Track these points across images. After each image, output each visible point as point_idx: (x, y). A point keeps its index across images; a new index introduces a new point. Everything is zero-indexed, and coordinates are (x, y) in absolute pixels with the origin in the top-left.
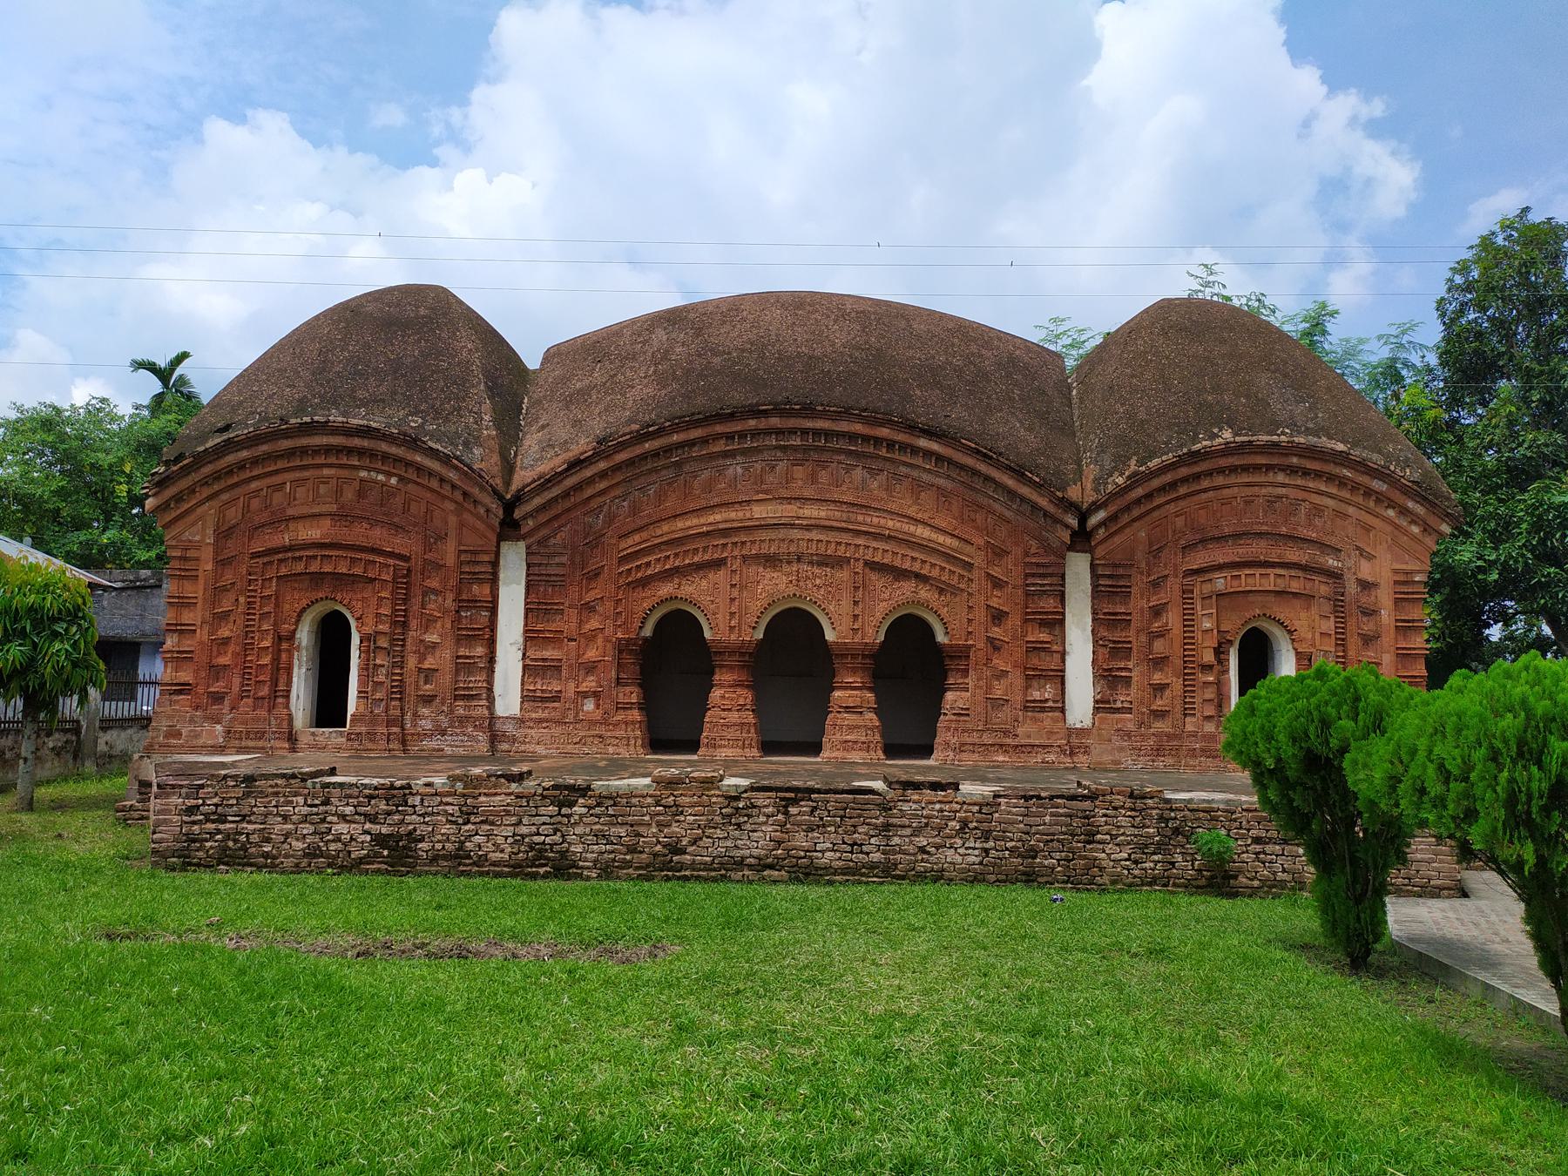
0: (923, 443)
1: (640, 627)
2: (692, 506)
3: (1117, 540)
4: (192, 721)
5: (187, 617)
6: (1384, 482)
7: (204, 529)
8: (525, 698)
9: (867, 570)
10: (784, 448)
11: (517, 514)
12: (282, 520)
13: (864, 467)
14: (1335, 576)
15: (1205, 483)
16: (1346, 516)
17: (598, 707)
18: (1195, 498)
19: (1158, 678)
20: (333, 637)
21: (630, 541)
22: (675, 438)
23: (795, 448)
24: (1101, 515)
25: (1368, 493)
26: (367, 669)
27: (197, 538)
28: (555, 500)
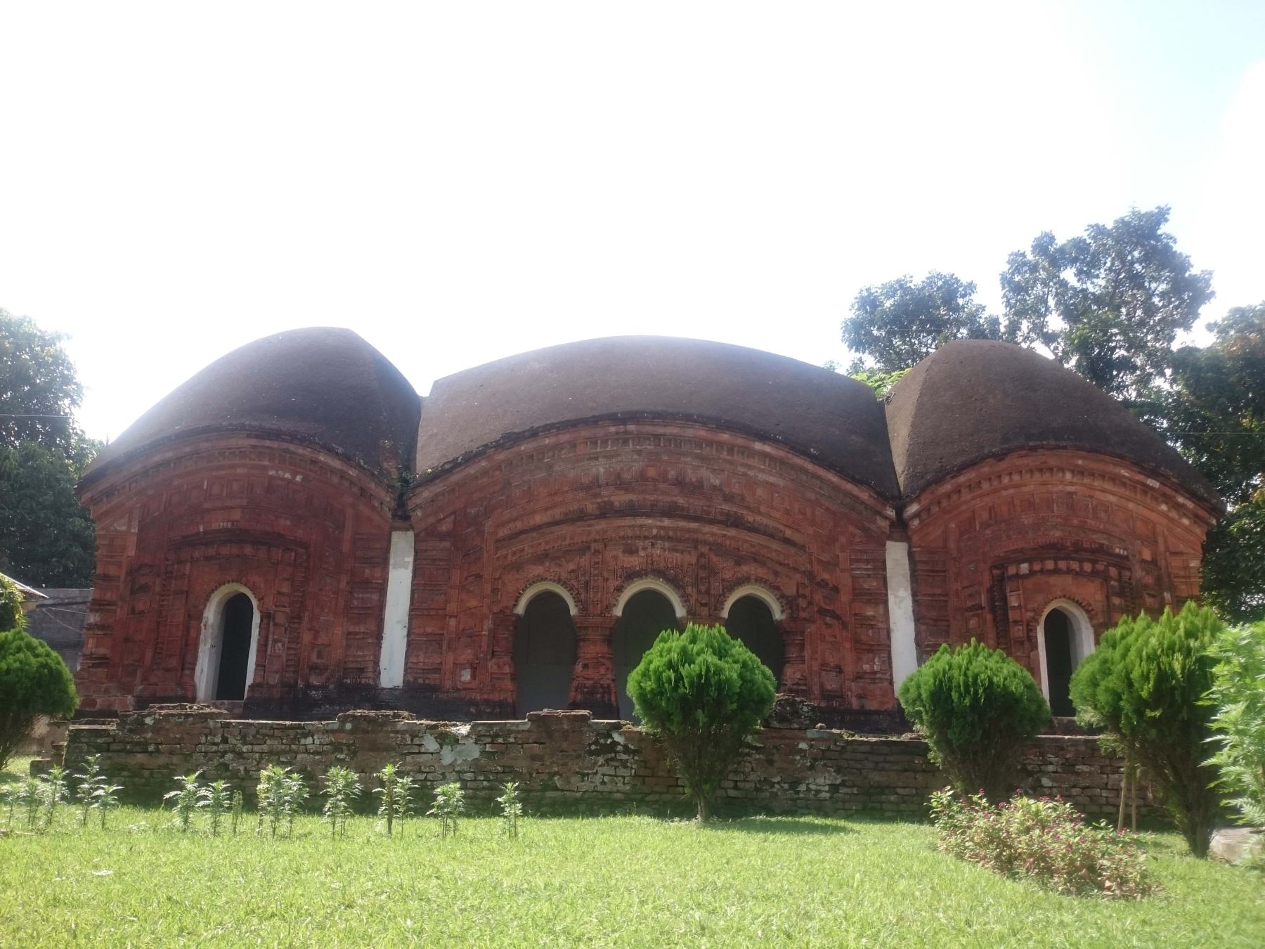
0: (758, 446)
1: (515, 606)
6: (1158, 481)
7: (130, 521)
8: (407, 669)
9: (712, 556)
11: (410, 505)
13: (707, 468)
14: (1122, 563)
16: (1126, 509)
17: (474, 677)
22: (547, 441)
24: (914, 508)
25: (1146, 489)
26: (266, 645)
27: (124, 528)
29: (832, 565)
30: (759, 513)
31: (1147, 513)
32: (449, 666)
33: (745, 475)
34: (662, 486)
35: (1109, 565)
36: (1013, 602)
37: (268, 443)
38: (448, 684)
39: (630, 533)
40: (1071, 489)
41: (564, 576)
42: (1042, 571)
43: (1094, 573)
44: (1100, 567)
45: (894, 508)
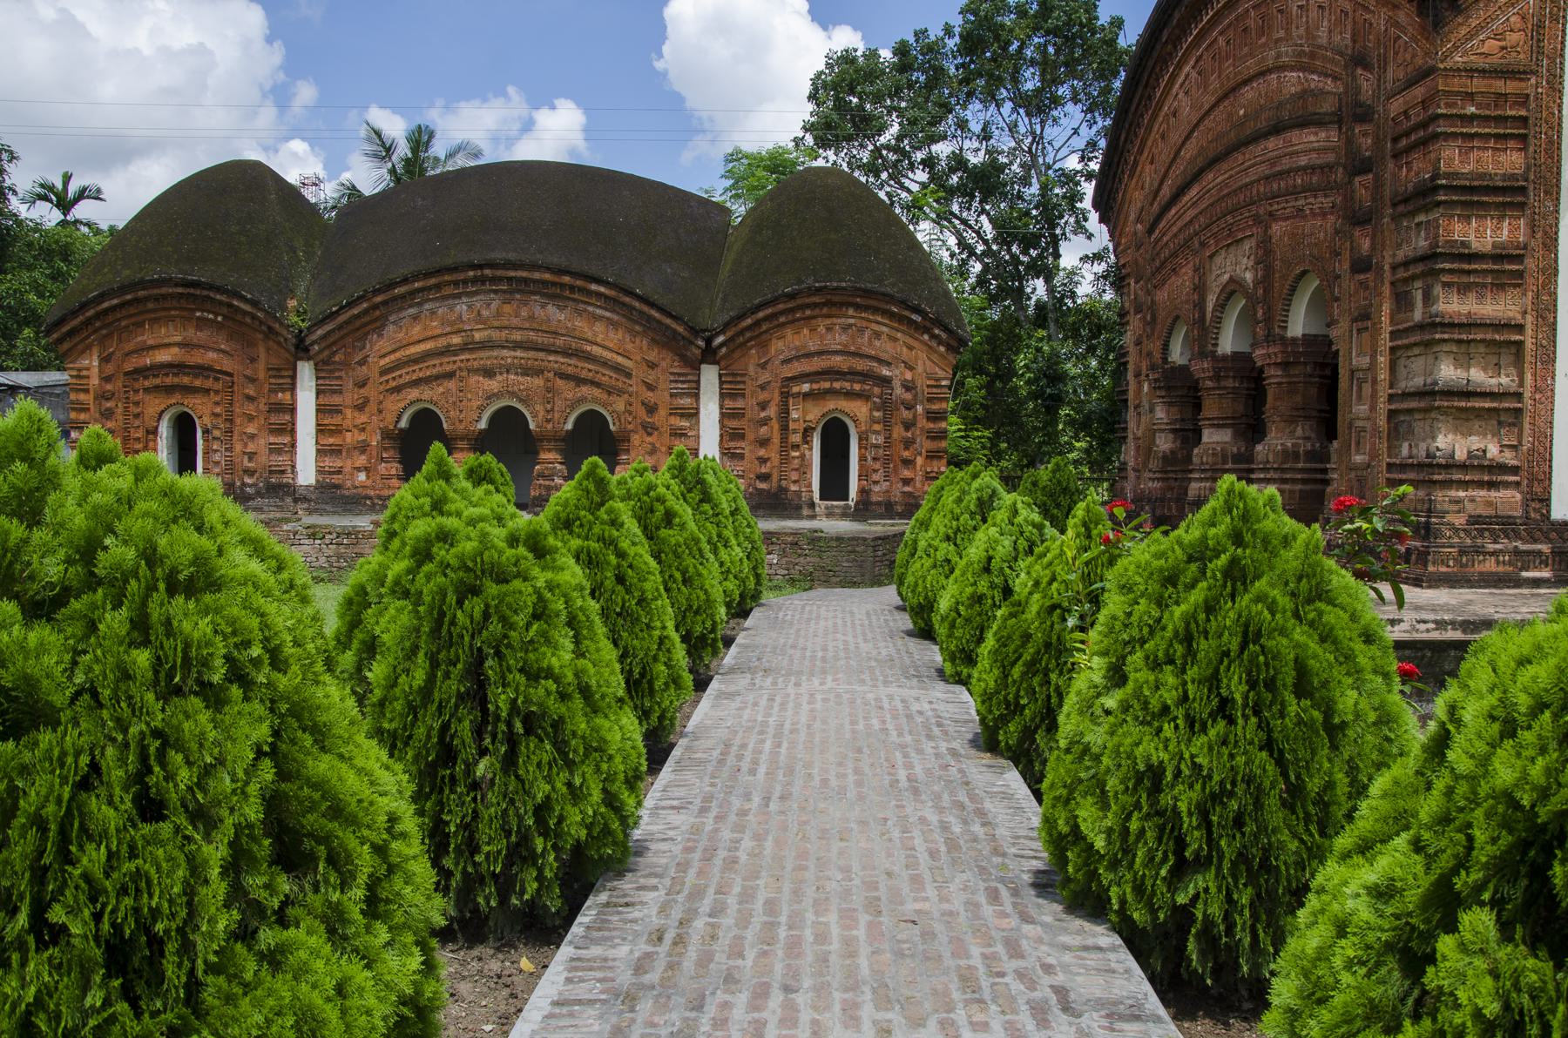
0: (594, 287)
2: (430, 334)
11: (308, 342)
14: (886, 382)
19: (762, 452)
21: (387, 360)
23: (504, 292)
24: (721, 339)
25: (911, 322)
28: (333, 331)
36: (794, 415)
38: (349, 483)
40: (852, 321)
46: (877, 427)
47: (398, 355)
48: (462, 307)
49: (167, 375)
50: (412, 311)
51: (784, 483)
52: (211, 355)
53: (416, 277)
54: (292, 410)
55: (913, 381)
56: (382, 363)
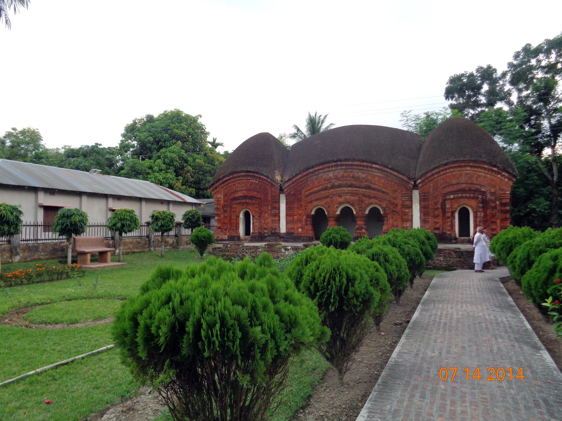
0: (374, 166)
2: (321, 183)
3: (425, 186)
4: (221, 235)
5: (219, 212)
10: (342, 169)
11: (283, 188)
12: (236, 192)
14: (484, 193)
15: (448, 171)
16: (487, 177)
17: (302, 230)
18: (445, 175)
19: (436, 220)
20: (247, 215)
23: (344, 169)
24: (419, 181)
25: (493, 171)
29: (395, 198)
30: (375, 185)
31: (493, 178)
32: (296, 228)
33: (371, 174)
34: (348, 178)
35: (479, 194)
36: (448, 206)
37: (249, 174)
38: (296, 232)
39: (340, 192)
40: (469, 172)
41: (323, 204)
42: (457, 197)
43: (473, 198)
44: (476, 195)
45: (413, 181)
46: (481, 210)
47: (311, 191)
48: (331, 174)
49: (242, 199)
50: (316, 177)
51: (444, 231)
52: (255, 193)
53: (316, 166)
54: (279, 209)
55: (494, 193)
56: (307, 193)
